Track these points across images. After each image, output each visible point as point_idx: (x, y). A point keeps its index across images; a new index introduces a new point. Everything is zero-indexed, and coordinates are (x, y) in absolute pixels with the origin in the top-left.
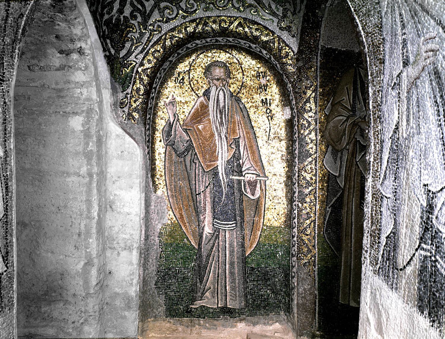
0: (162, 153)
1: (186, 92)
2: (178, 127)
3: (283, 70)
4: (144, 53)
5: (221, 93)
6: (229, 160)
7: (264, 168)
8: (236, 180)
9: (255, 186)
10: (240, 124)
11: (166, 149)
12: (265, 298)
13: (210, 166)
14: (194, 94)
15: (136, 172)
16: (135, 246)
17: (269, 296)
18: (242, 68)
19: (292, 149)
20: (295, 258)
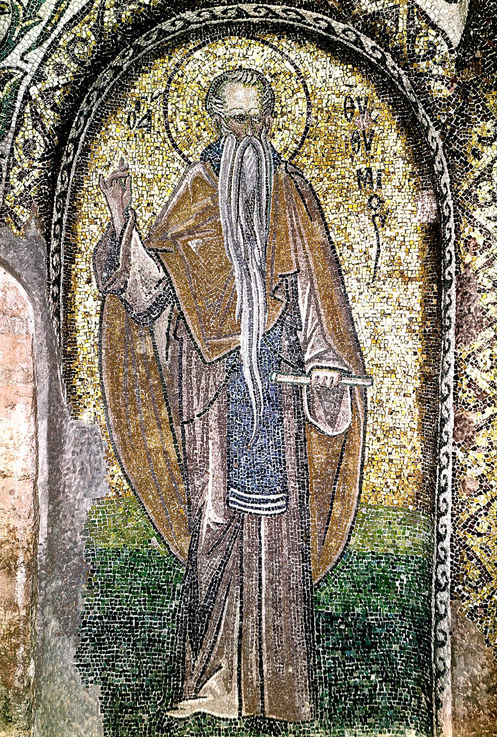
0: (93, 313)
1: (157, 152)
3: (418, 93)
4: (45, 45)
5: (249, 152)
6: (268, 332)
10: (298, 238)
11: (104, 302)
12: (364, 695)
13: (219, 346)
14: (179, 157)
15: (24, 366)
16: (21, 559)
17: (375, 690)
18: (305, 86)
19: (438, 304)
20: (445, 596)
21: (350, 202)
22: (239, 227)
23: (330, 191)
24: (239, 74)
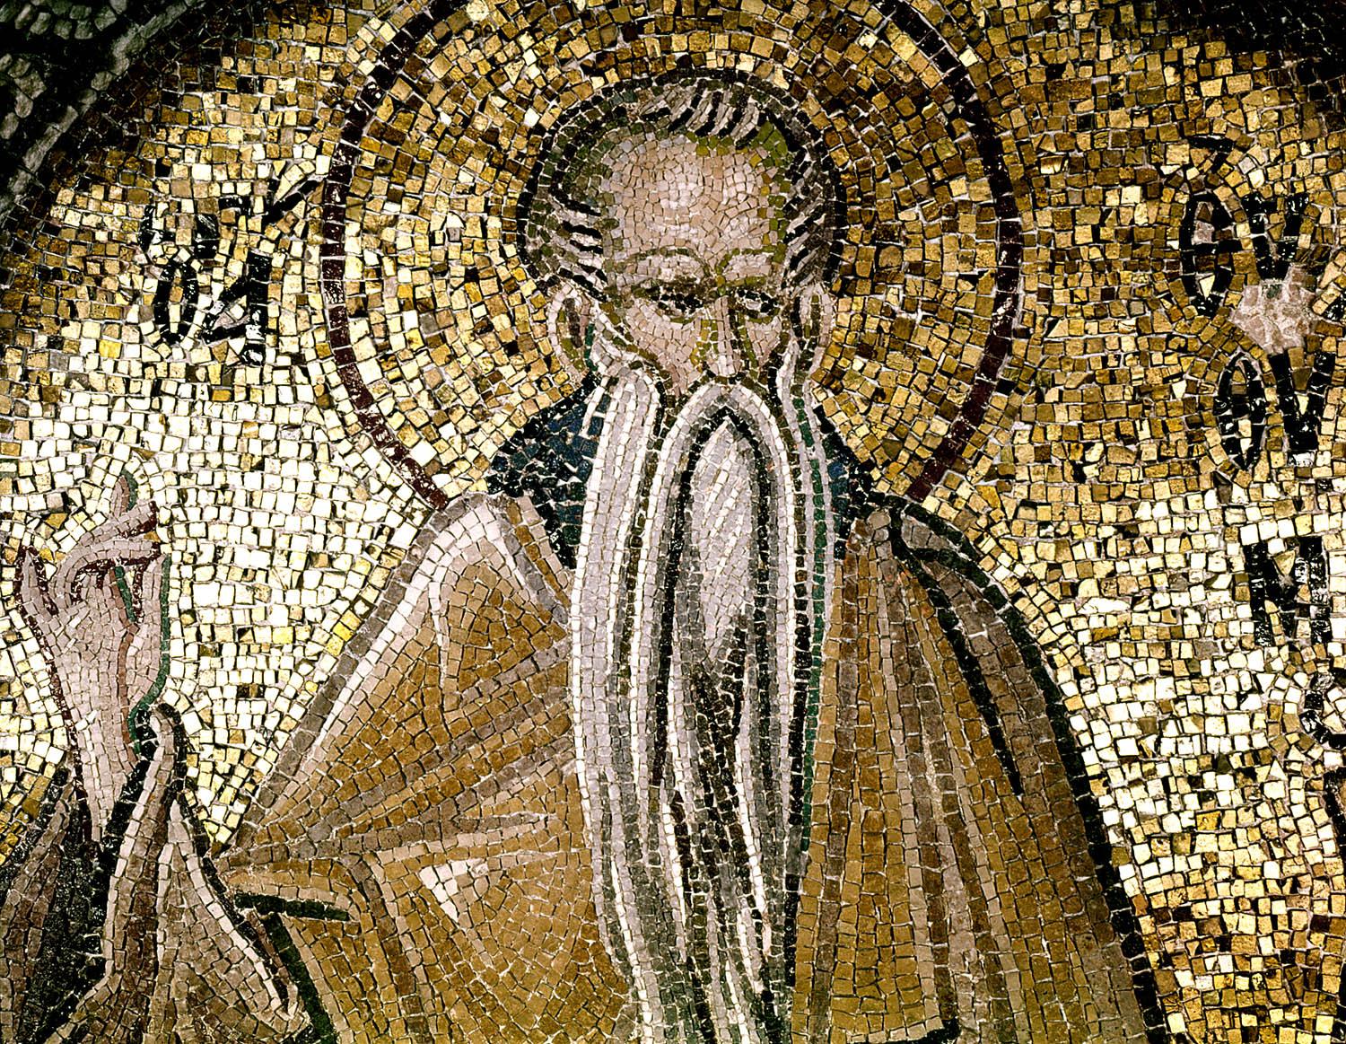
5: (723, 459)
10: (954, 886)
18: (989, 148)
24: (677, 100)
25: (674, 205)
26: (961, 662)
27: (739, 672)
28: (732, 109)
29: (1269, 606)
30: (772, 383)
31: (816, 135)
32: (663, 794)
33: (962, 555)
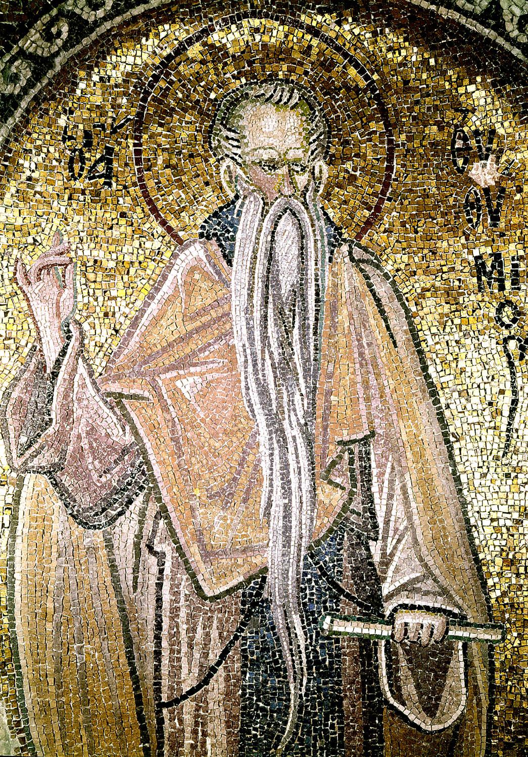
1: (123, 221)
2: (84, 386)
5: (286, 225)
6: (318, 543)
7: (484, 584)
8: (351, 637)
9: (442, 668)
14: (160, 229)
21: (464, 314)
22: (267, 356)
23: (428, 294)
25: (267, 130)
26: (375, 299)
27: (294, 305)
28: (289, 94)
29: (483, 278)
30: (305, 198)
31: (320, 105)
32: (267, 351)
33: (375, 261)
